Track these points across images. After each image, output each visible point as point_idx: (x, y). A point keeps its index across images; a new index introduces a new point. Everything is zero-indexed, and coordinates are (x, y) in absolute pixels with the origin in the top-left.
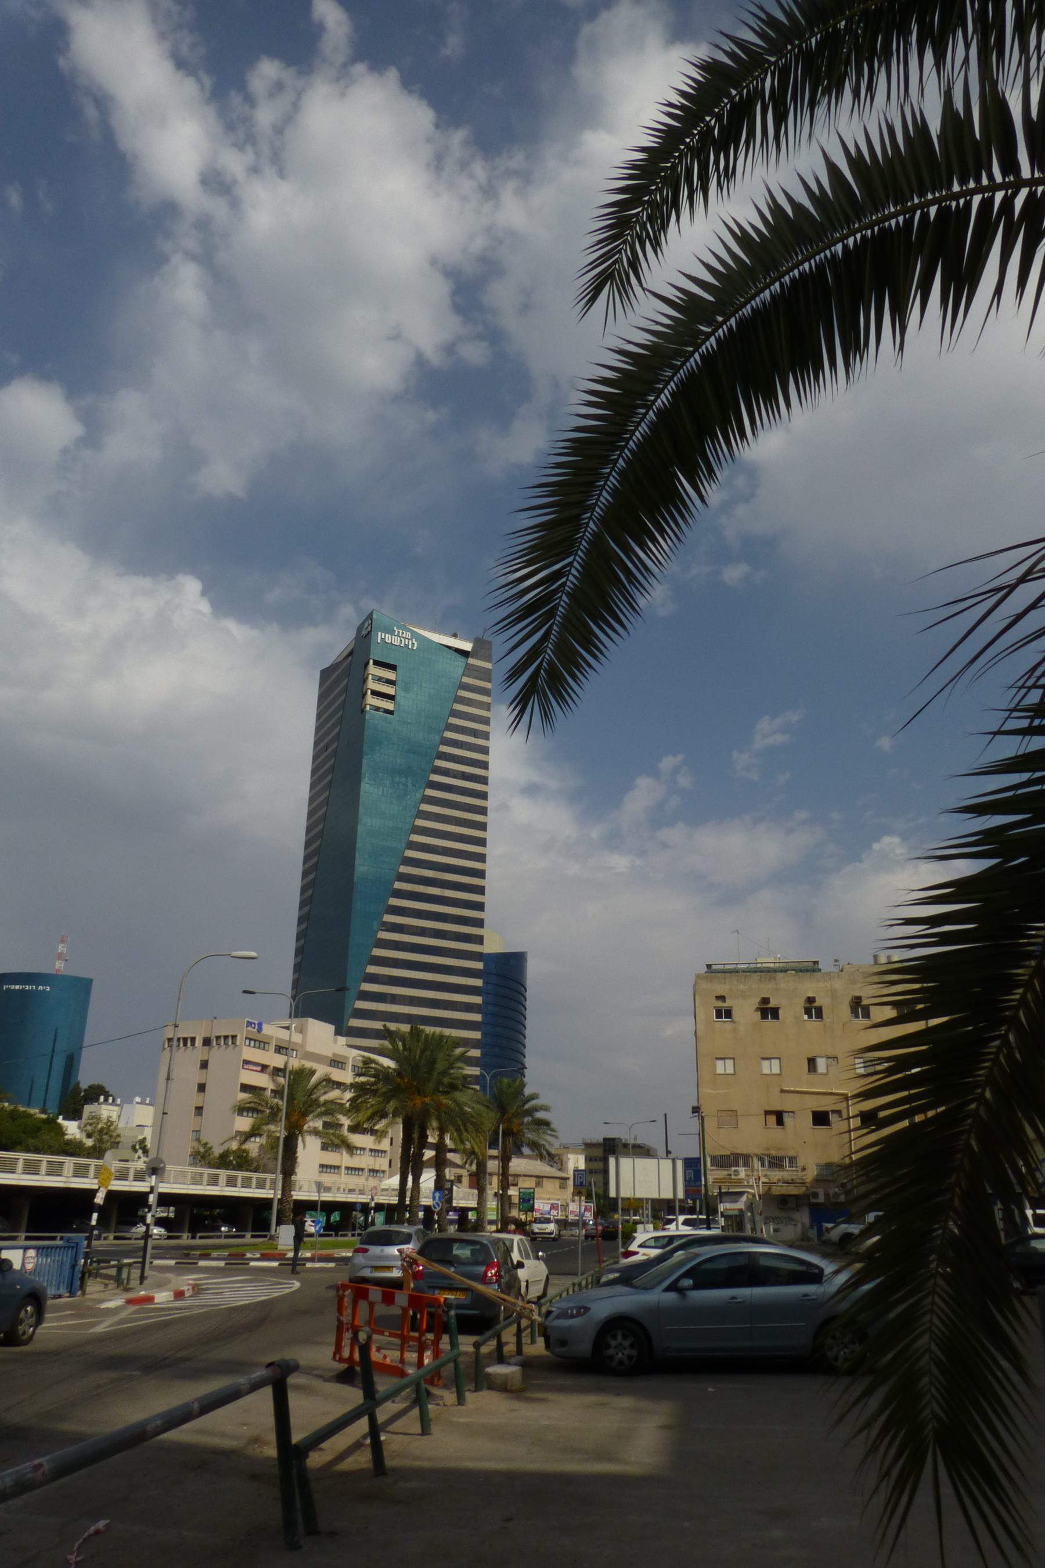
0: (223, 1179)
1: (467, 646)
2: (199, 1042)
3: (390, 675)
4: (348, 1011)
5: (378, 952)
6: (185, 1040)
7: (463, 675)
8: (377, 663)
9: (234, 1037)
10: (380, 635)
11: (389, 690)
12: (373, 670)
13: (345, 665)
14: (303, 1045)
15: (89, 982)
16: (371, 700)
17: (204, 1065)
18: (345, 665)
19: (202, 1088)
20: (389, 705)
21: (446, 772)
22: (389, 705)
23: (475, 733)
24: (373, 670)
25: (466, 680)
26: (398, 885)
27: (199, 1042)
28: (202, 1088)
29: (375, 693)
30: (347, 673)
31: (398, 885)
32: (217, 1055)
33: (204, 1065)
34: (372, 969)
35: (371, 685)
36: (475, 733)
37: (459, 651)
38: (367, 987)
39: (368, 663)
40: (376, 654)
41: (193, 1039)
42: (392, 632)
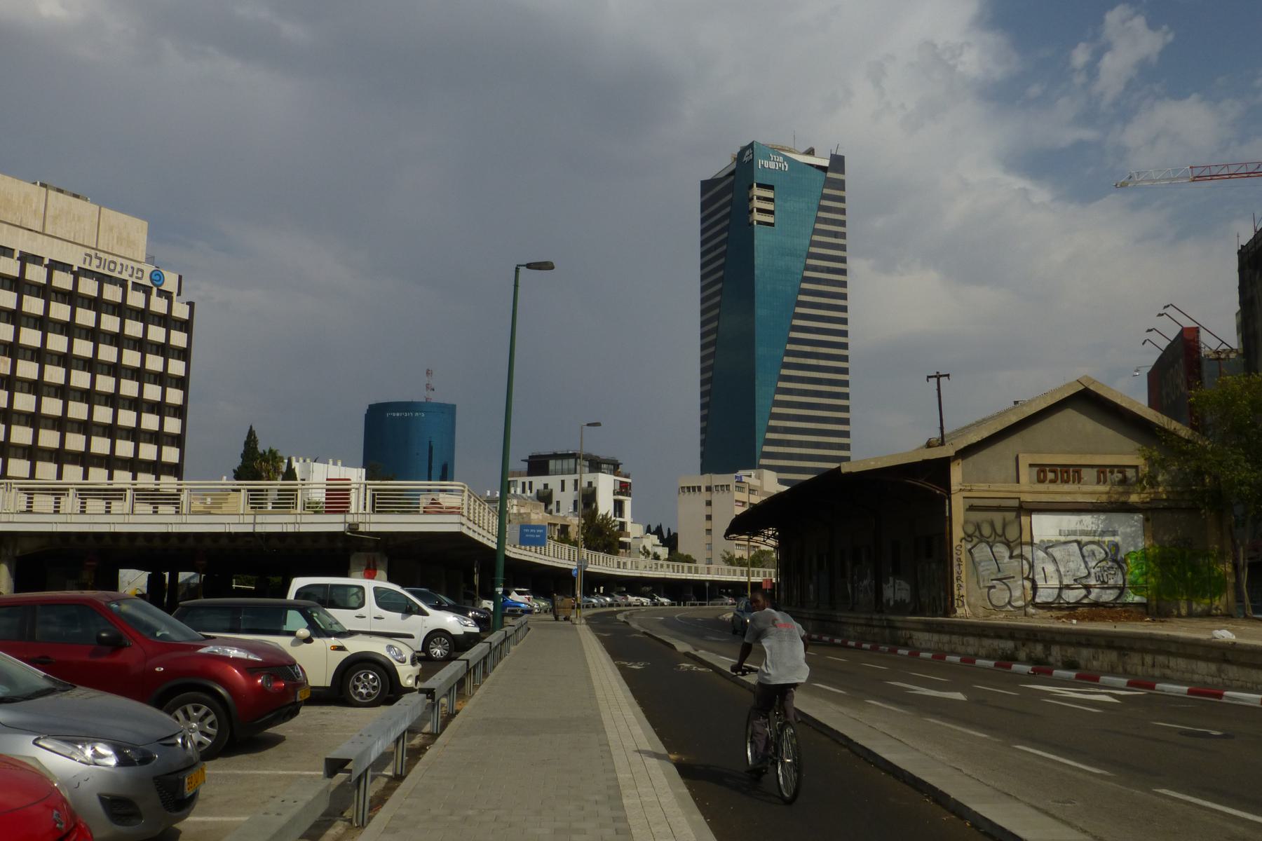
0: (712, 571)
1: (826, 163)
2: (703, 489)
3: (770, 194)
4: (758, 454)
5: (776, 410)
6: (694, 488)
7: (824, 187)
8: (759, 186)
9: (728, 486)
10: (760, 163)
11: (770, 207)
12: (757, 192)
13: (726, 183)
14: (762, 487)
15: (454, 406)
16: (757, 217)
17: (709, 503)
18: (726, 183)
19: (709, 518)
20: (769, 219)
21: (815, 269)
22: (769, 219)
23: (836, 235)
24: (757, 192)
25: (826, 191)
26: (786, 359)
27: (703, 489)
28: (709, 518)
29: (759, 210)
30: (729, 188)
31: (786, 359)
32: (716, 497)
33: (709, 503)
34: (772, 423)
35: (757, 204)
36: (836, 235)
37: (819, 167)
38: (770, 436)
39: (752, 186)
40: (758, 178)
41: (699, 488)
42: (769, 159)
